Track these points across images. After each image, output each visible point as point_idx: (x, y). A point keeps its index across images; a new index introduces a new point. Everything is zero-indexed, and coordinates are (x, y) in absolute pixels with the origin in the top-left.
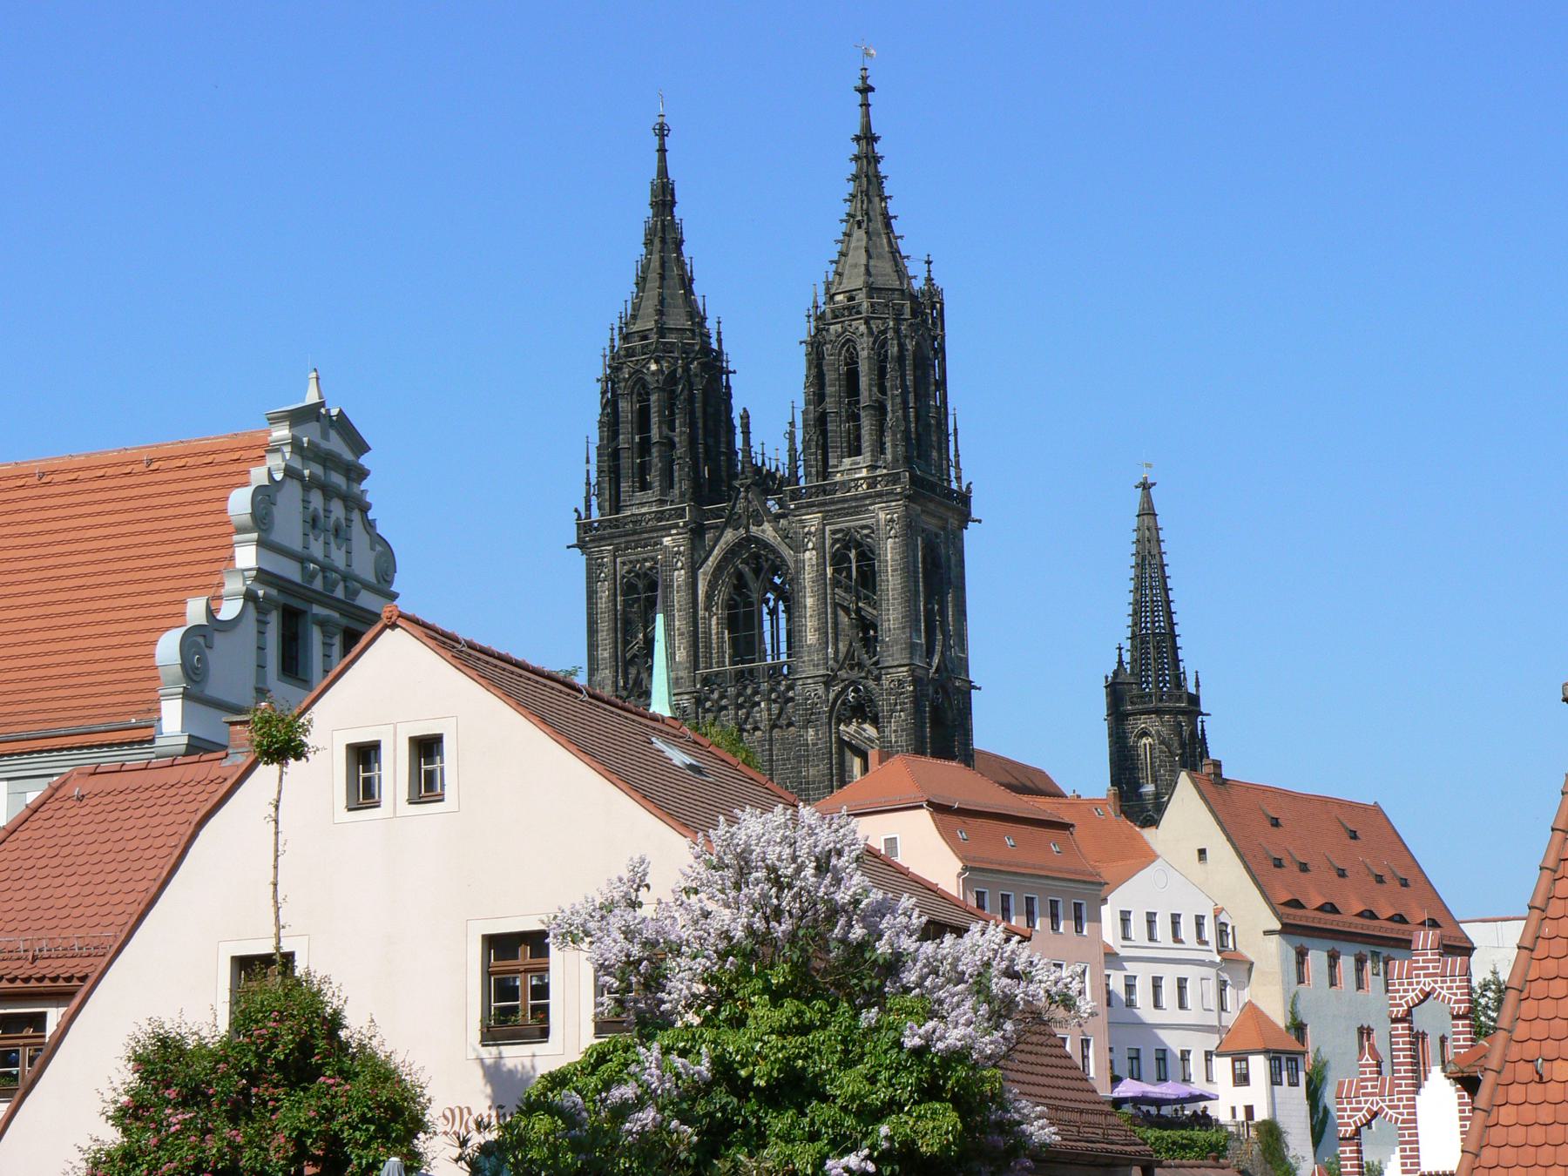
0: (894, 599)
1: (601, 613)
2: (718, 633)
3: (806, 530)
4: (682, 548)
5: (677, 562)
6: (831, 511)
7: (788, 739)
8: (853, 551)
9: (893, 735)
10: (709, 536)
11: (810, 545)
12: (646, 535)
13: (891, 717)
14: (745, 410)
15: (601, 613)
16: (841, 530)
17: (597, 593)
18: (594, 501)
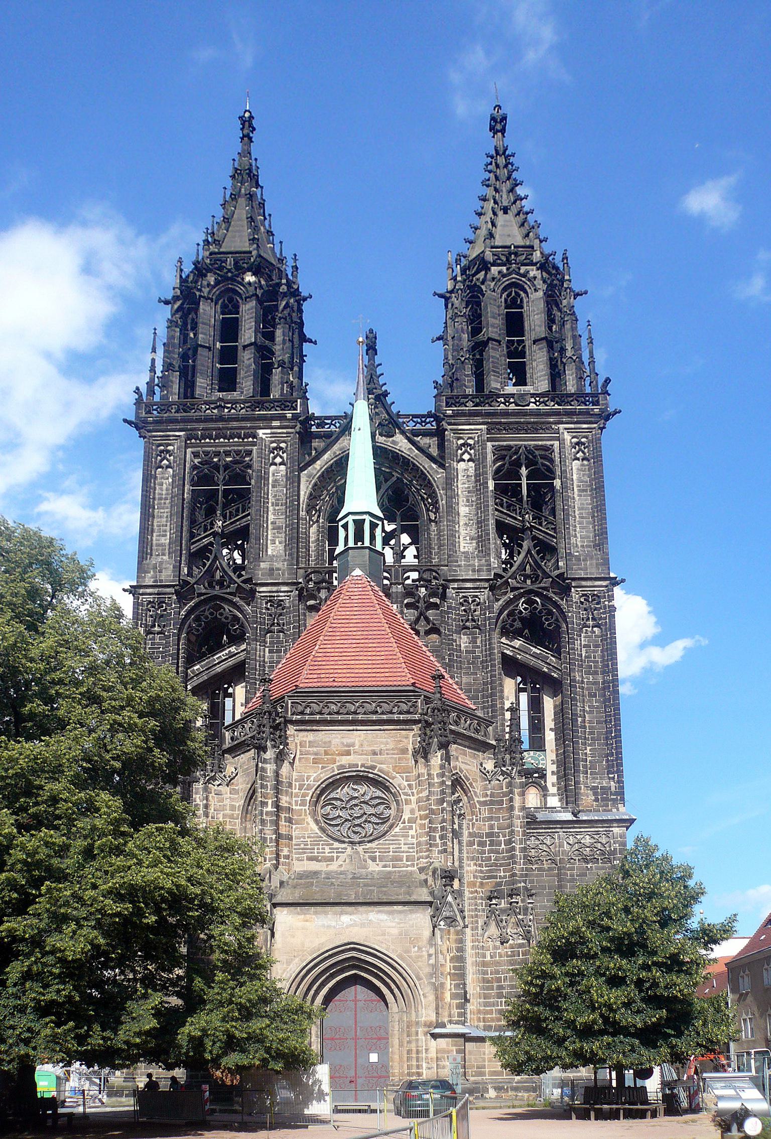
3: (461, 442)
5: (275, 458)
6: (500, 423)
8: (524, 468)
10: (316, 443)
12: (235, 424)
14: (371, 331)
16: (509, 448)
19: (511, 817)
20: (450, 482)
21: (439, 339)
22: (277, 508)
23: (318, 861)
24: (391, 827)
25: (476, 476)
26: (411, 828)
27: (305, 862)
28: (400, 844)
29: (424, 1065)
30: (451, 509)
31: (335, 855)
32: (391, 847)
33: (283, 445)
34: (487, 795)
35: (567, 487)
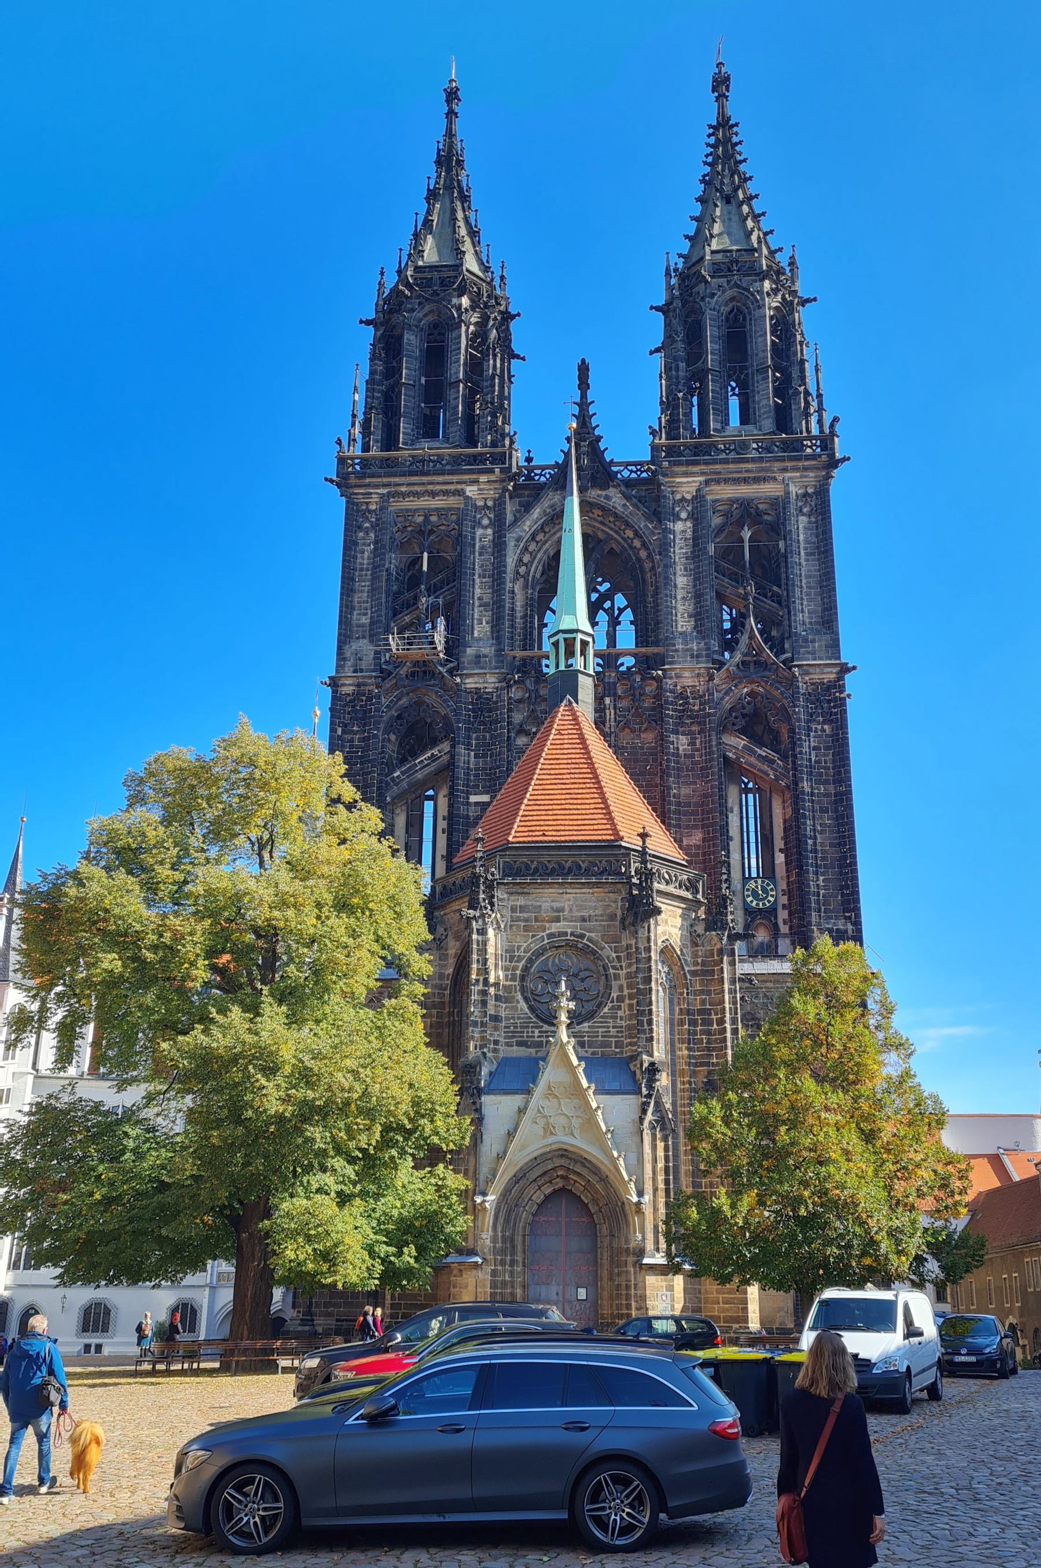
0: (809, 587)
1: (362, 570)
2: (525, 616)
3: (678, 497)
4: (490, 503)
7: (642, 748)
8: (746, 528)
9: (813, 753)
11: (684, 515)
13: (809, 729)
15: (362, 570)
17: (356, 544)
18: (358, 436)
19: (723, 991)
20: (665, 547)
21: (657, 350)
22: (484, 580)
23: (528, 1047)
24: (600, 1006)
25: (695, 538)
26: (619, 1007)
27: (515, 1048)
28: (608, 1027)
29: (633, 1304)
30: (668, 582)
31: (544, 1040)
32: (600, 1030)
33: (490, 503)
34: (698, 964)
35: (791, 552)
